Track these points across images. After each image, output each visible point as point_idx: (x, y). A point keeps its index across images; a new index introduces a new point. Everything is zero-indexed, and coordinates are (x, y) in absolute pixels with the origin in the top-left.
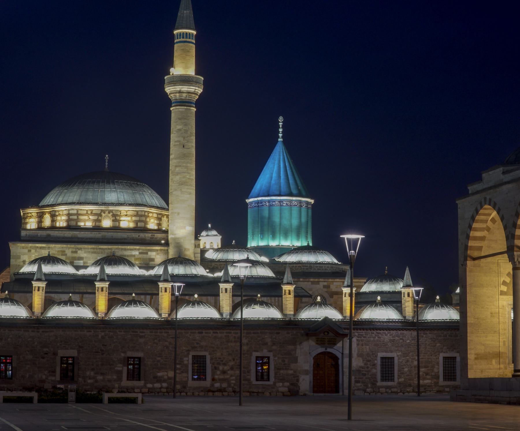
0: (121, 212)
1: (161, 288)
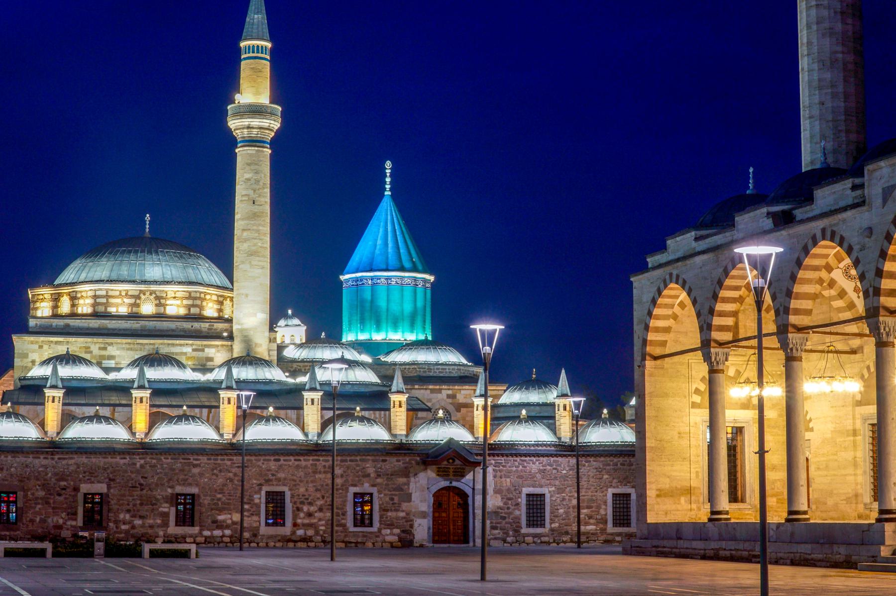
0: (166, 293)
1: (223, 398)
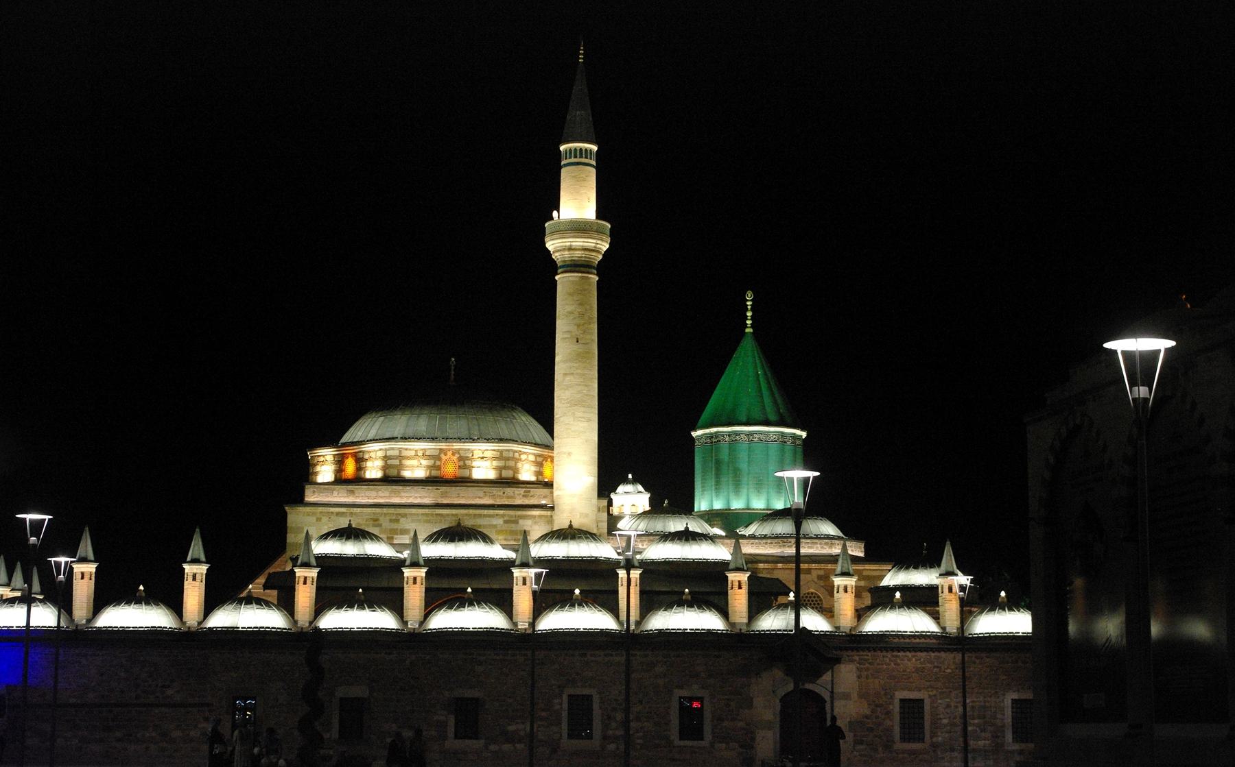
0: (473, 452)
1: (517, 577)
